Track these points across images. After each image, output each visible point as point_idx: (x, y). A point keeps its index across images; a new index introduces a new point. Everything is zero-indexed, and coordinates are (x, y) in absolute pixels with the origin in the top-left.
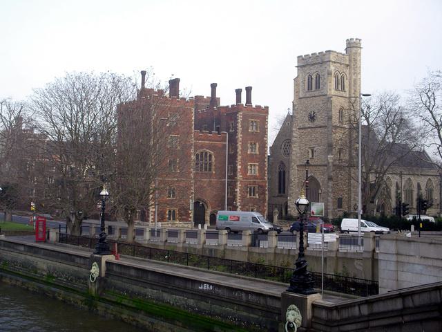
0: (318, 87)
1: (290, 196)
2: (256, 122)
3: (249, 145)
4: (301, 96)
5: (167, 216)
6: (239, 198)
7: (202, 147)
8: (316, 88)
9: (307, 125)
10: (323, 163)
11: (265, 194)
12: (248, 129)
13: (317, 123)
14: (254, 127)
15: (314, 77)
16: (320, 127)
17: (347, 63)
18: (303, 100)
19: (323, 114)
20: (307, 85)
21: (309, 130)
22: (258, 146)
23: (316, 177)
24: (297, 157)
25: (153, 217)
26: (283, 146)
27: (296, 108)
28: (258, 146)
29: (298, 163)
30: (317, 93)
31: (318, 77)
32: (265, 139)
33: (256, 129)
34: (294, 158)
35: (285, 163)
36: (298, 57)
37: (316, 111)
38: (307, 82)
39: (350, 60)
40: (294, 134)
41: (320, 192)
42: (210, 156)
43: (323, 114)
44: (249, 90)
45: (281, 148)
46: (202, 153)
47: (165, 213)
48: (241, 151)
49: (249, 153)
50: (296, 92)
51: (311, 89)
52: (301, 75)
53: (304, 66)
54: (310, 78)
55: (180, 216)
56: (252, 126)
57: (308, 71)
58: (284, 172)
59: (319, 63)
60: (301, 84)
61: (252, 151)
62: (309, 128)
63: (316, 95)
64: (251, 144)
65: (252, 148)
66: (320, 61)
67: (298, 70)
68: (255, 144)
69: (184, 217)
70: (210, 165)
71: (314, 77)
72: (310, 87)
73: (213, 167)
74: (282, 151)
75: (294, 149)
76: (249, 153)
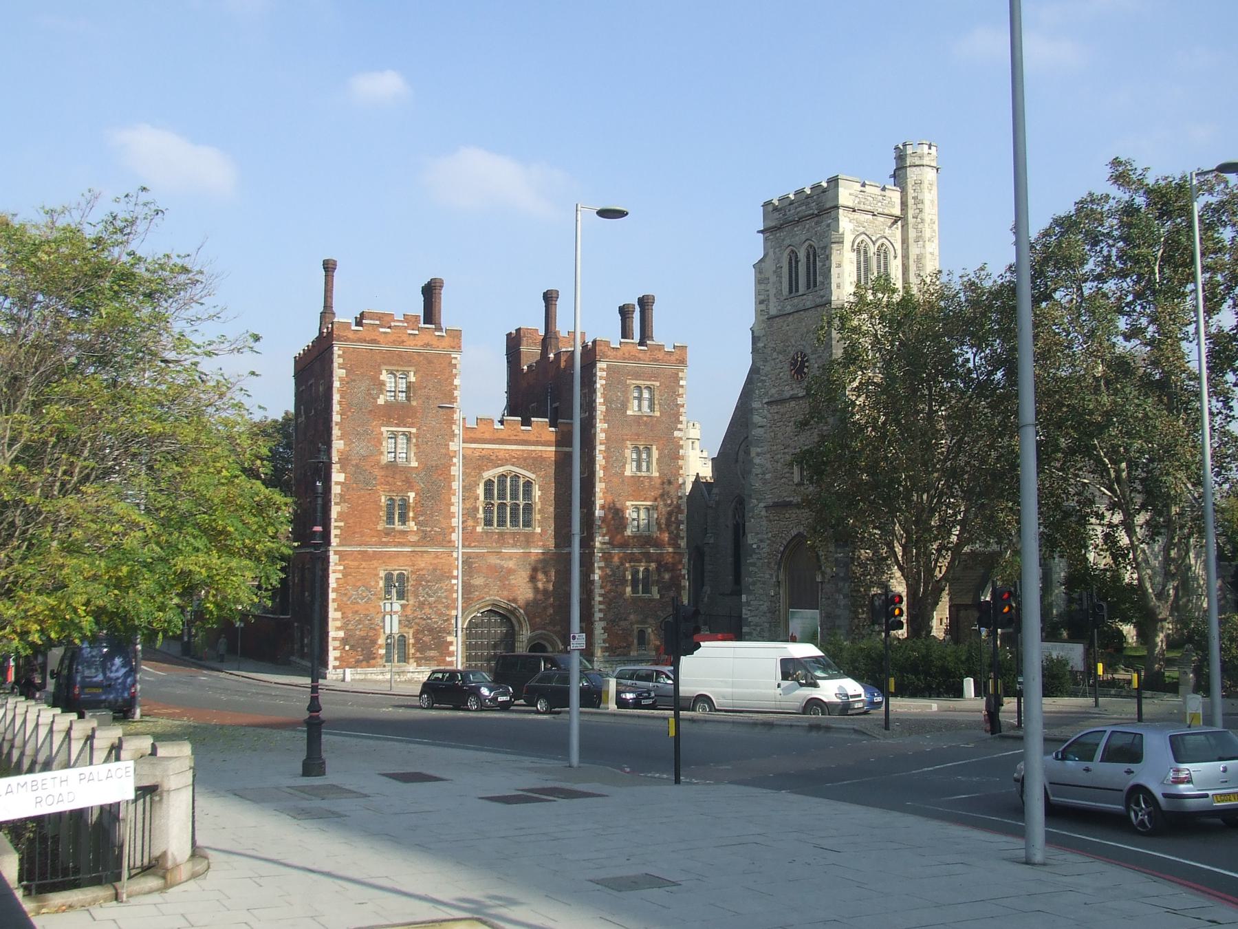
1: (750, 592)
2: (648, 388)
3: (628, 453)
4: (773, 312)
5: (382, 651)
6: (598, 599)
7: (493, 461)
8: (808, 288)
11: (679, 588)
12: (624, 407)
14: (645, 404)
15: (802, 255)
17: (897, 211)
21: (793, 404)
22: (655, 454)
24: (765, 482)
25: (337, 654)
27: (761, 345)
28: (655, 454)
29: (770, 499)
32: (676, 434)
33: (651, 407)
34: (758, 485)
37: (808, 351)
39: (904, 204)
40: (757, 419)
42: (528, 484)
44: (645, 303)
46: (502, 477)
47: (374, 642)
48: (605, 468)
49: (628, 473)
50: (761, 301)
54: (793, 260)
55: (417, 650)
56: (640, 399)
57: (787, 242)
59: (813, 216)
60: (773, 279)
61: (639, 468)
63: (809, 304)
64: (636, 448)
65: (639, 462)
67: (766, 240)
68: (648, 449)
69: (432, 653)
70: (528, 508)
71: (802, 255)
73: (537, 517)
75: (757, 460)
76: (628, 473)
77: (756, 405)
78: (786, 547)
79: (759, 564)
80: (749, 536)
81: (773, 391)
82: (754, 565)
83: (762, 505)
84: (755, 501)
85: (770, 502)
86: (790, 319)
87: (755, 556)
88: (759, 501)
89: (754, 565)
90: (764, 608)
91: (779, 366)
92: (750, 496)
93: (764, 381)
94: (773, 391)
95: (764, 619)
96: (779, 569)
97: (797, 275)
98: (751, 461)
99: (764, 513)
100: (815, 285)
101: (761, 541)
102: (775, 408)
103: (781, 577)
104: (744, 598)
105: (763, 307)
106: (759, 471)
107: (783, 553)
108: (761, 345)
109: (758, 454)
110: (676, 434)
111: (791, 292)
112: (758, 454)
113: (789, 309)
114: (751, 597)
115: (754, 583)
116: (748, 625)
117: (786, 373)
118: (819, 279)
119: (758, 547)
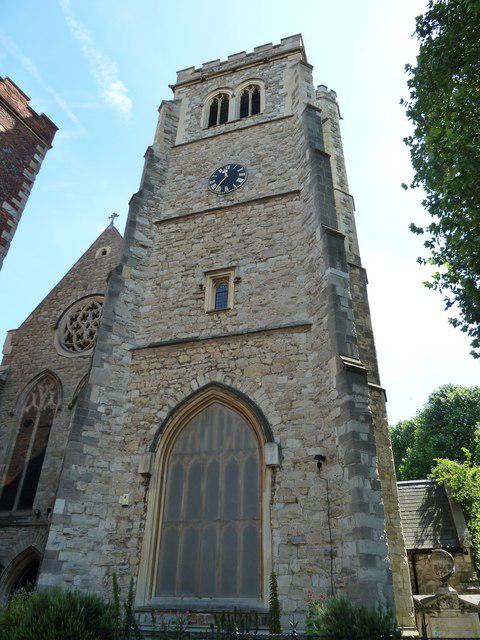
1: (73, 494)
4: (179, 140)
8: (244, 113)
10: (286, 322)
13: (245, 193)
16: (264, 200)
18: (184, 151)
19: (277, 164)
21: (209, 218)
26: (66, 320)
27: (158, 166)
30: (249, 121)
34: (125, 314)
35: (61, 374)
37: (245, 162)
41: (271, 456)
45: (56, 327)
52: (186, 101)
58: (49, 414)
74: (57, 337)
75: (130, 284)
78: (172, 413)
79: (103, 442)
80: (95, 391)
82: (93, 442)
83: (128, 346)
84: (116, 338)
85: (142, 343)
87: (98, 427)
88: (125, 339)
89: (93, 442)
90: (101, 532)
92: (109, 328)
95: (91, 557)
96: (153, 449)
98: (121, 282)
99: (127, 359)
101: (115, 403)
102: (172, 227)
103: (157, 467)
104: (59, 506)
105: (169, 137)
106: (131, 298)
107: (164, 424)
109: (134, 278)
110: (6, 206)
111: (212, 123)
112: (134, 278)
114: (76, 507)
115: (87, 479)
116: (57, 570)
117: (201, 187)
119: (108, 412)
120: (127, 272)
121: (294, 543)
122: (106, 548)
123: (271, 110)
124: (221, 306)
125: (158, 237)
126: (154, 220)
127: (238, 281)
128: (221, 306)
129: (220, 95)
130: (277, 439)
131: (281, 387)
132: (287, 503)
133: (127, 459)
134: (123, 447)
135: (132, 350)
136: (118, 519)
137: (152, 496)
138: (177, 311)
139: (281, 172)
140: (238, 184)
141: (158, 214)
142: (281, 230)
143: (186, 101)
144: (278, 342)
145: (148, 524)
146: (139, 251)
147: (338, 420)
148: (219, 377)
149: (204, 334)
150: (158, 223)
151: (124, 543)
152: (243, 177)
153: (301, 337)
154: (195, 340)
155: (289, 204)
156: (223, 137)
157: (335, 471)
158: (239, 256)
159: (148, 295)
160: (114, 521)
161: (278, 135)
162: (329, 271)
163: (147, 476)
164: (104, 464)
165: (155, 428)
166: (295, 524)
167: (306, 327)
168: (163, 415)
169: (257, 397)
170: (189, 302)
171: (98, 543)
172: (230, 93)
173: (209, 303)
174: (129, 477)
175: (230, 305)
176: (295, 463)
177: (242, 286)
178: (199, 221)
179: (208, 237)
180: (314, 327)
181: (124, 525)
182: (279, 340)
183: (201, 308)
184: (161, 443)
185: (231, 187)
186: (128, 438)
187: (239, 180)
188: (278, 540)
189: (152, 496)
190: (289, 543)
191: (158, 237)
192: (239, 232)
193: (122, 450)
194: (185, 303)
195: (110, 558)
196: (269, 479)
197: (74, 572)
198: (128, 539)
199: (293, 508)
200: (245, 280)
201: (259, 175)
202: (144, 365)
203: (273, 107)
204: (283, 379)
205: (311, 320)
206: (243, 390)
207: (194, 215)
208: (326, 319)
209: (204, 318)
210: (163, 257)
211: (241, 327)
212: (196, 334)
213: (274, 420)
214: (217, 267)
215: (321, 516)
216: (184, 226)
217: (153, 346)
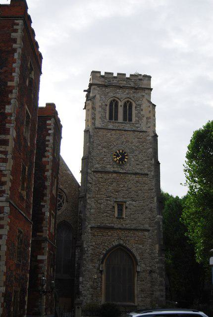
0: (128, 117)
1: (83, 276)
8: (125, 119)
9: (109, 168)
10: (142, 227)
13: (128, 168)
16: (136, 174)
18: (101, 133)
19: (140, 156)
20: (134, 112)
21: (115, 175)
23: (129, 247)
30: (127, 127)
31: (128, 107)
36: (93, 72)
38: (108, 108)
41: (139, 269)
43: (140, 156)
51: (116, 119)
53: (106, 86)
54: (114, 104)
59: (132, 88)
60: (98, 109)
62: (115, 172)
66: (132, 85)
71: (121, 104)
72: (113, 116)
75: (88, 201)
77: (89, 171)
78: (108, 252)
81: (97, 165)
83: (90, 226)
85: (93, 225)
86: (113, 132)
88: (89, 223)
90: (88, 286)
91: (103, 153)
92: (85, 220)
93: (92, 159)
94: (97, 165)
96: (102, 263)
97: (117, 112)
98: (86, 200)
100: (130, 120)
102: (100, 175)
104: (81, 279)
107: (105, 255)
108: (92, 140)
111: (111, 118)
112: (89, 198)
113: (111, 127)
115: (85, 271)
118: (134, 119)
120: (88, 196)
121: (142, 291)
122: (91, 290)
123: (137, 122)
124: (120, 217)
125: (94, 178)
126: (92, 170)
127: (126, 208)
128: (120, 217)
129: (114, 100)
130: (139, 264)
131: (140, 249)
132: (141, 281)
133: (94, 265)
134: (92, 261)
135: (91, 227)
136: (93, 282)
137: (103, 277)
138: (105, 214)
139: (141, 161)
140: (125, 162)
141: (93, 166)
142: (141, 190)
143: (98, 96)
144: (140, 234)
145: (103, 284)
146: (89, 185)
147: (157, 263)
148: (122, 242)
149: (115, 226)
150: (94, 171)
151: (96, 289)
152: (127, 159)
153: (146, 233)
154: (112, 228)
155: (144, 179)
156: (118, 132)
157: (155, 275)
158: (126, 197)
159: (93, 204)
160: (92, 283)
161: (141, 140)
162: (158, 216)
163: (101, 272)
164: (88, 266)
165: (102, 256)
166: (143, 286)
167: (148, 231)
168: (104, 252)
169: (133, 250)
170: (108, 212)
171: (88, 289)
172: (120, 104)
173: (116, 215)
174: (95, 270)
175: (124, 216)
176: (144, 271)
177: (128, 210)
178: (110, 175)
179: (114, 184)
180: (151, 231)
181: (95, 284)
182: (140, 233)
183: (114, 215)
184: (105, 261)
185: (122, 163)
186: (93, 258)
187: (126, 160)
188: (139, 290)
189: (103, 277)
190: (142, 291)
191: (94, 178)
192: (126, 185)
193: (91, 261)
194: (108, 212)
195: (92, 293)
196: (137, 275)
197: (85, 296)
198: (98, 287)
199: (143, 282)
200: (129, 207)
201: (133, 159)
202: (96, 234)
203: (138, 121)
204: (141, 246)
205: (150, 228)
206: (129, 248)
207: (109, 172)
208: (156, 231)
209: (115, 219)
210: (97, 189)
211: (127, 226)
212: (113, 225)
213: (138, 258)
214: (119, 200)
215: (149, 285)
216: (106, 176)
217: (99, 228)
